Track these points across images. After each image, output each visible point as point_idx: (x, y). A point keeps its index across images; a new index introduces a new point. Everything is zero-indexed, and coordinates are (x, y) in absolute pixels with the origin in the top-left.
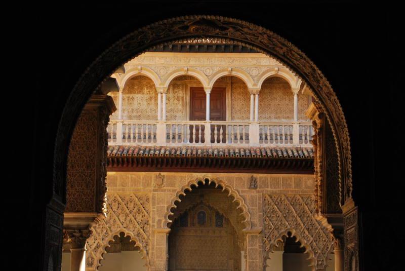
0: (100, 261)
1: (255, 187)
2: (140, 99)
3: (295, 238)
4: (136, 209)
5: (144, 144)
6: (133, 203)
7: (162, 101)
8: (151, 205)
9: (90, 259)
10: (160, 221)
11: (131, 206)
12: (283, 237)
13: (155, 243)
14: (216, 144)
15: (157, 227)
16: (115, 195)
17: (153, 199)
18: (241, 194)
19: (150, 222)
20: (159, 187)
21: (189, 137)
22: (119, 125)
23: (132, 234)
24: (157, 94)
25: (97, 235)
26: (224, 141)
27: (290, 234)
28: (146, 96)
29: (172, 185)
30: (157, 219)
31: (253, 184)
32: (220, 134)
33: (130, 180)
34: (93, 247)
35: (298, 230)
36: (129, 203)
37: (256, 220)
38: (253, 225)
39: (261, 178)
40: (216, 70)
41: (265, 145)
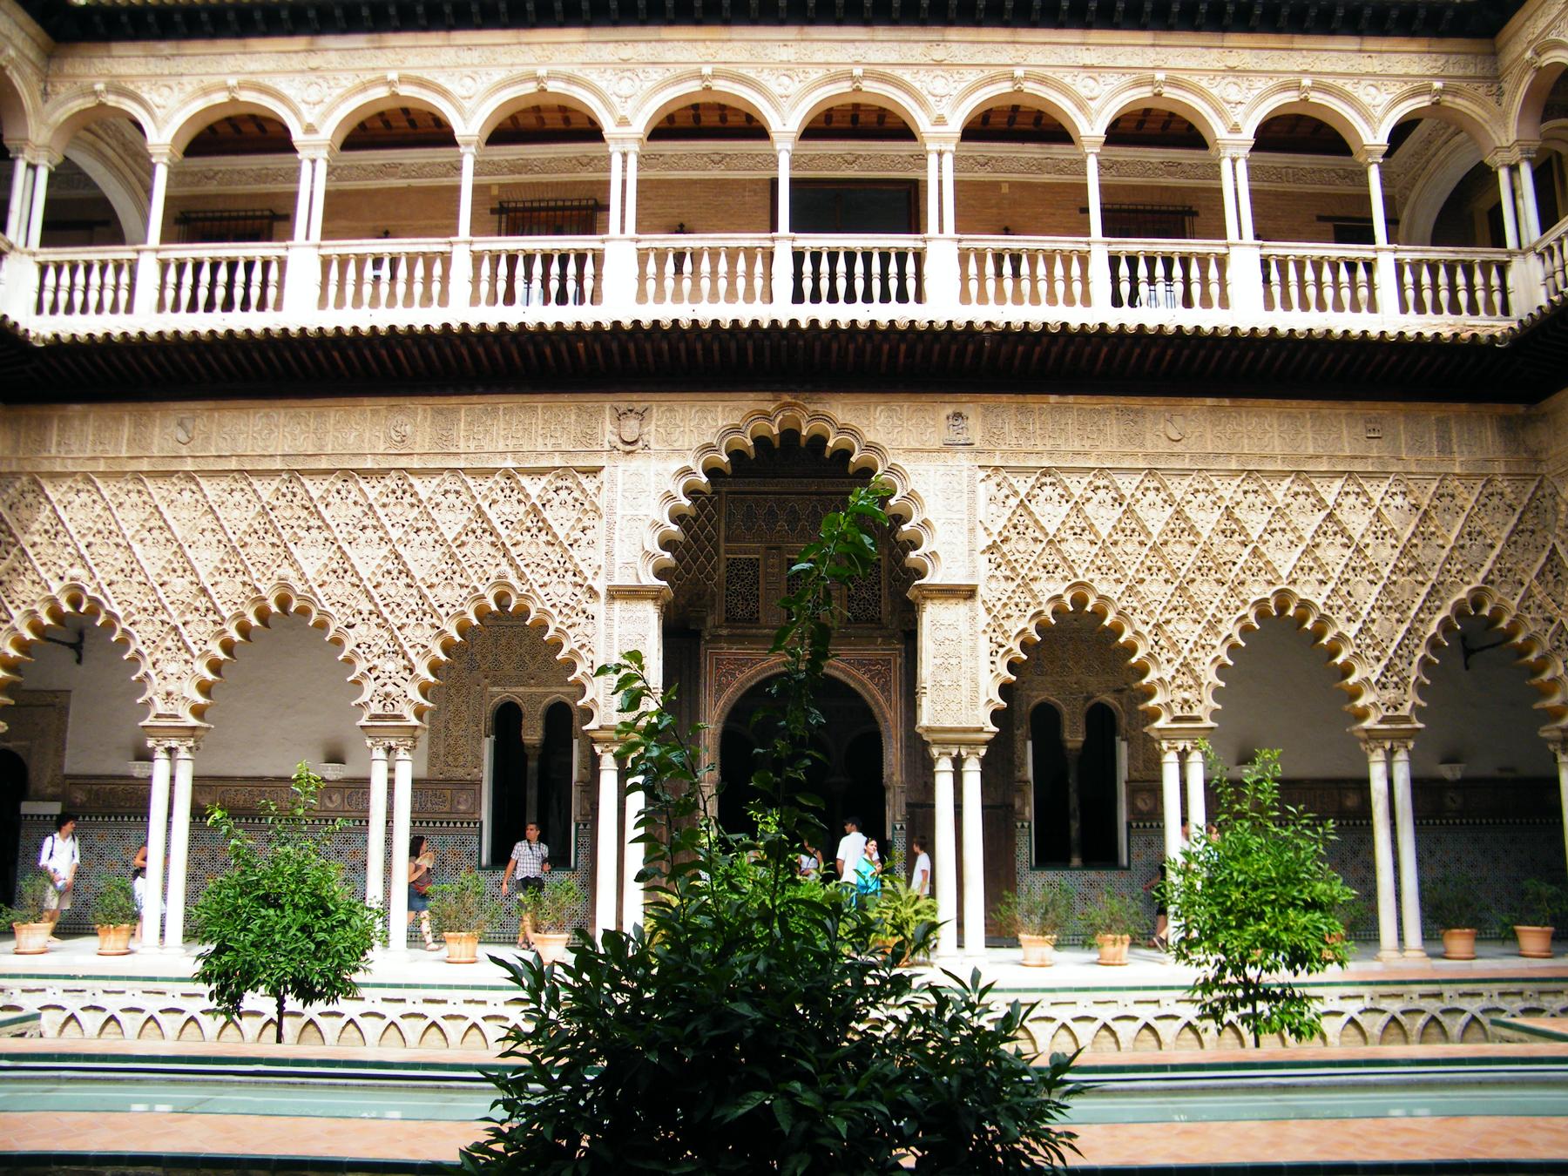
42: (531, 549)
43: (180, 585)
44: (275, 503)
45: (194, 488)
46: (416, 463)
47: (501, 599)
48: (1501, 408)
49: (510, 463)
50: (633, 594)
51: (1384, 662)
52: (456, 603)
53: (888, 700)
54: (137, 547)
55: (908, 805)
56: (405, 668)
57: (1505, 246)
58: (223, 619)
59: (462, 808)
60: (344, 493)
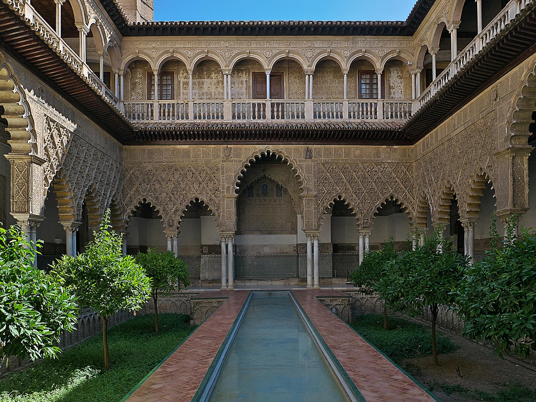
0: (179, 222)
1: (311, 157)
2: (209, 83)
3: (344, 201)
6: (205, 172)
7: (227, 86)
8: (221, 173)
12: (335, 200)
14: (275, 120)
17: (223, 169)
18: (298, 163)
20: (227, 158)
21: (252, 114)
22: (191, 104)
23: (205, 200)
24: (223, 76)
26: (283, 118)
27: (340, 197)
28: (215, 81)
29: (238, 156)
31: (309, 155)
32: (278, 110)
34: (173, 210)
35: (347, 194)
37: (312, 187)
38: (308, 190)
39: (315, 149)
40: (275, 52)
41: (318, 120)
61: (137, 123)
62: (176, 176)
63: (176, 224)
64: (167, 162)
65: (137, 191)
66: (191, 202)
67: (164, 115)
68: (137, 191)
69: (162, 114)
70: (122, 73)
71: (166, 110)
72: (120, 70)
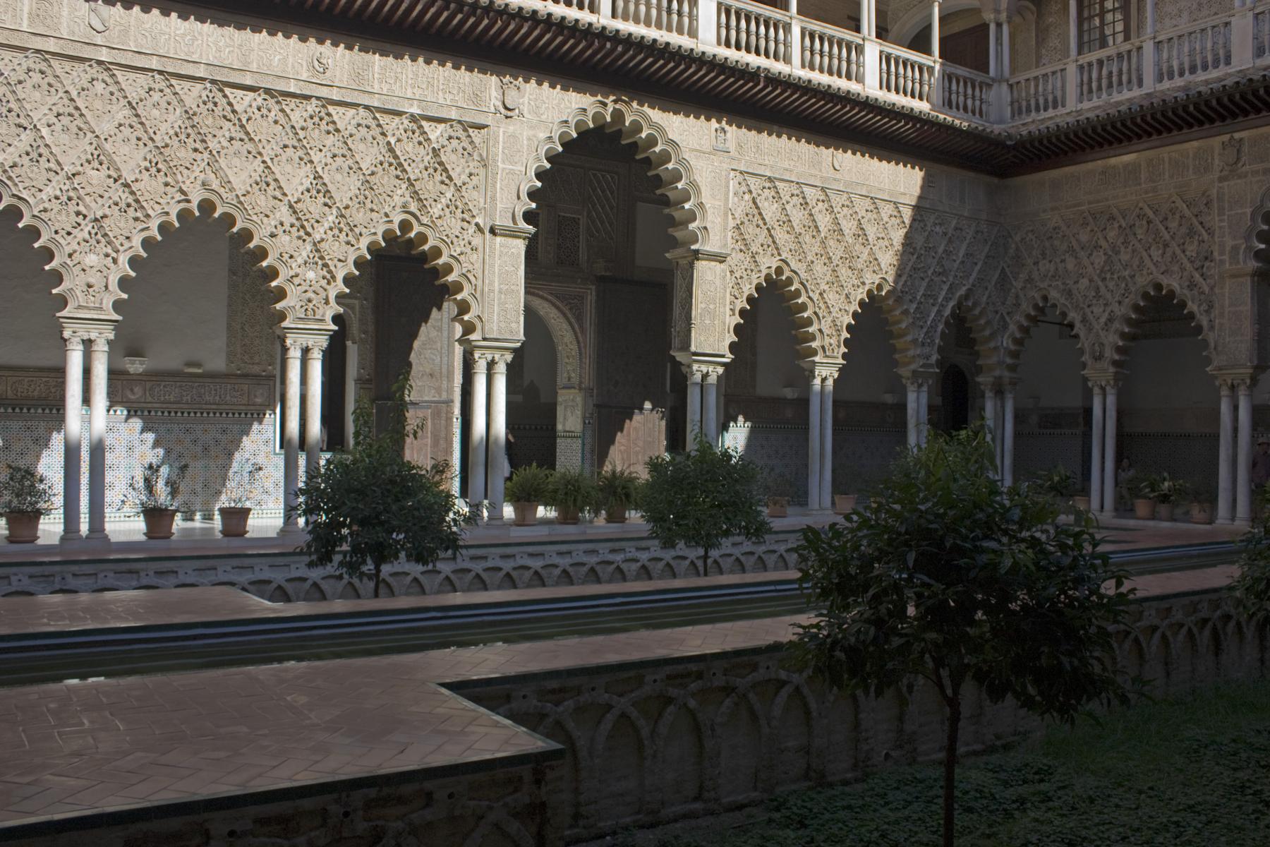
4: (1184, 230)
5: (1201, 76)
6: (1177, 216)
9: (1097, 348)
10: (1235, 249)
11: (1173, 225)
13: (1227, 302)
15: (1231, 264)
16: (1141, 205)
19: (1216, 254)
22: (1148, 48)
25: (1109, 296)
30: (1230, 243)
33: (1167, 165)
34: (1103, 320)
36: (1170, 217)
42: (429, 187)
43: (96, 177)
44: (196, 109)
45: (109, 80)
46: (335, 95)
47: (405, 226)
48: (987, 178)
49: (415, 110)
50: (512, 234)
51: (925, 330)
52: (372, 231)
53: (581, 327)
54: (45, 131)
55: (597, 406)
56: (324, 278)
57: (987, 72)
58: (148, 216)
59: (259, 400)
60: (264, 111)
61: (1033, 122)
62: (1111, 234)
63: (1110, 354)
64: (1090, 203)
65: (1030, 280)
66: (1146, 296)
67: (1090, 91)
68: (1030, 280)
69: (1085, 88)
70: (1003, 16)
71: (1095, 75)
72: (997, 11)
